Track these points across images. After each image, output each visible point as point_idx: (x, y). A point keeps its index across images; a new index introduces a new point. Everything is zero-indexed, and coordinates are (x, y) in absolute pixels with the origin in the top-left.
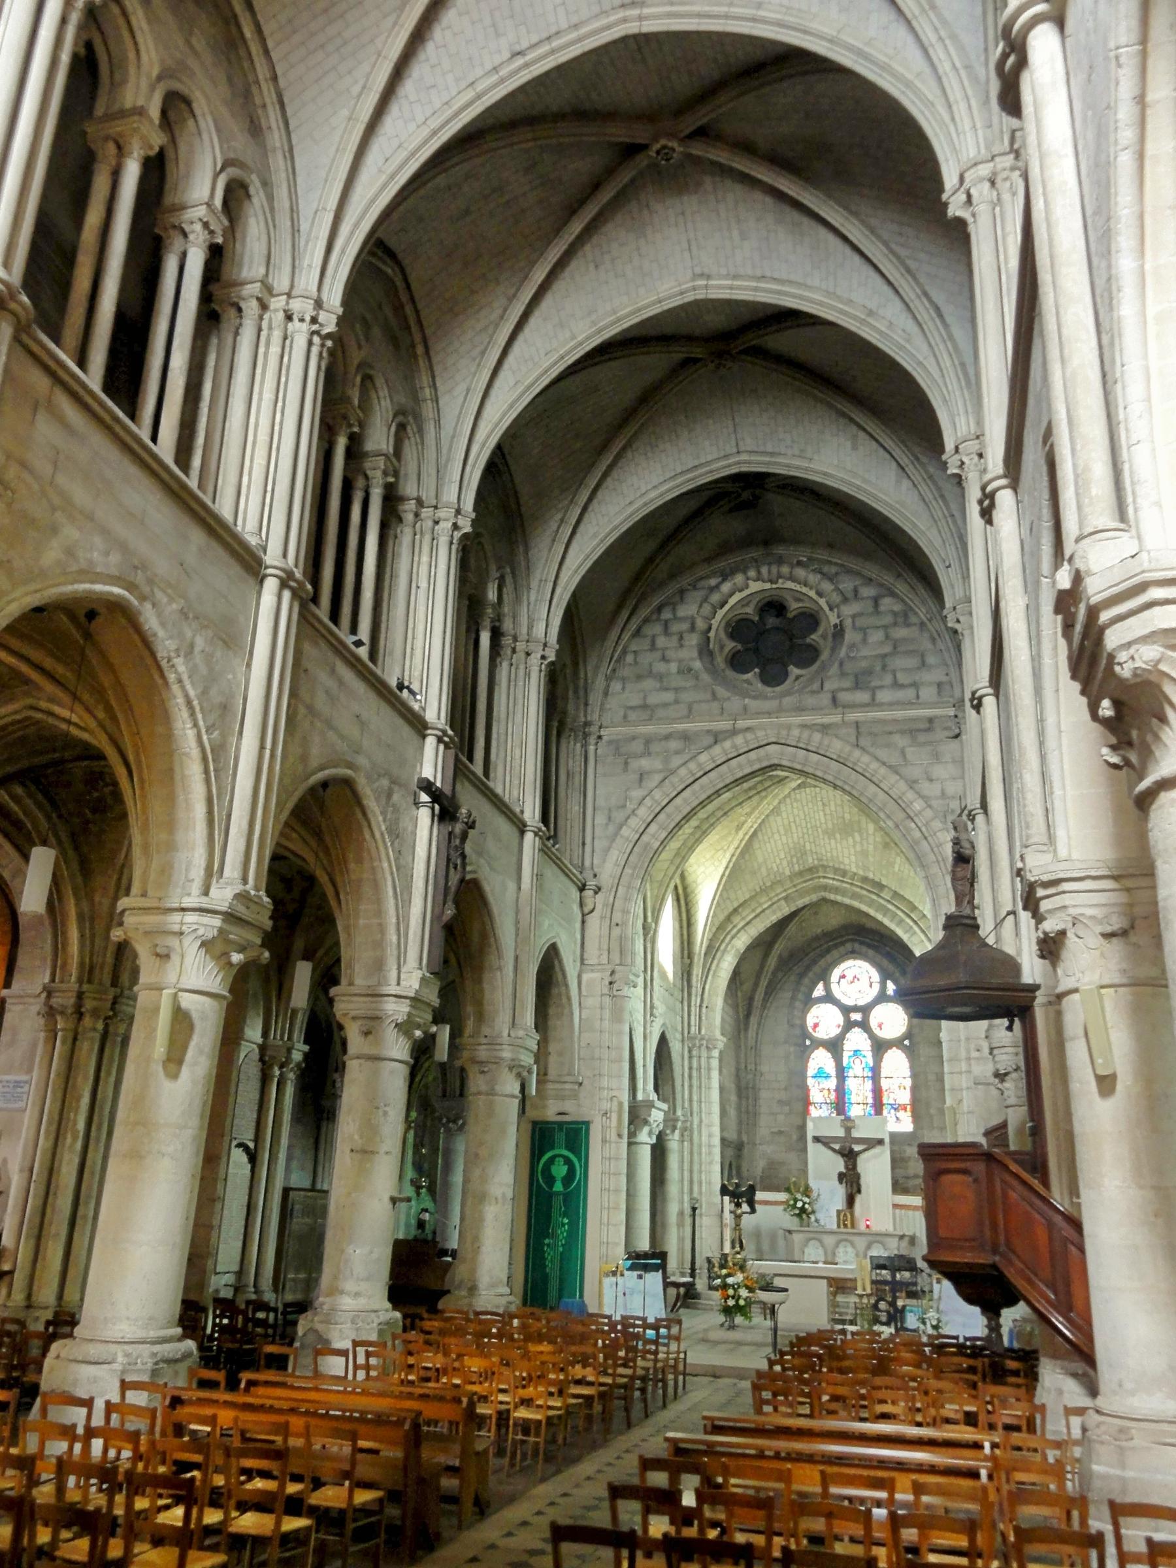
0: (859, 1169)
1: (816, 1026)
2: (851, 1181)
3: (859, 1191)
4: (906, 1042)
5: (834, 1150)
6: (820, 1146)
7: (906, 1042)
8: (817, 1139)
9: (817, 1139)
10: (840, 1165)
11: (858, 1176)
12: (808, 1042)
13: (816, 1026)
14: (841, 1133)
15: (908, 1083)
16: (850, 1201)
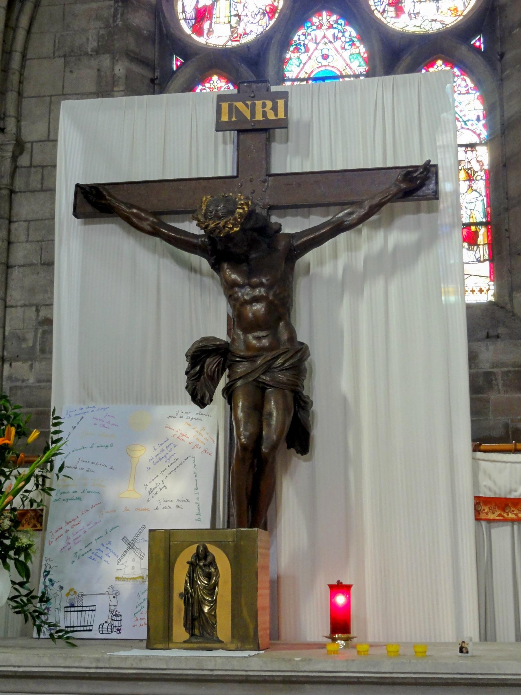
0: (308, 322)
1: (202, 15)
2: (265, 397)
3: (299, 438)
4: (478, 42)
5: (182, 242)
6: (112, 237)
7: (478, 42)
8: (95, 202)
9: (95, 202)
10: (200, 307)
11: (297, 359)
12: (176, 62)
13: (202, 15)
14: (215, 158)
15: (483, 156)
16: (251, 486)
